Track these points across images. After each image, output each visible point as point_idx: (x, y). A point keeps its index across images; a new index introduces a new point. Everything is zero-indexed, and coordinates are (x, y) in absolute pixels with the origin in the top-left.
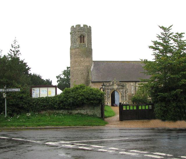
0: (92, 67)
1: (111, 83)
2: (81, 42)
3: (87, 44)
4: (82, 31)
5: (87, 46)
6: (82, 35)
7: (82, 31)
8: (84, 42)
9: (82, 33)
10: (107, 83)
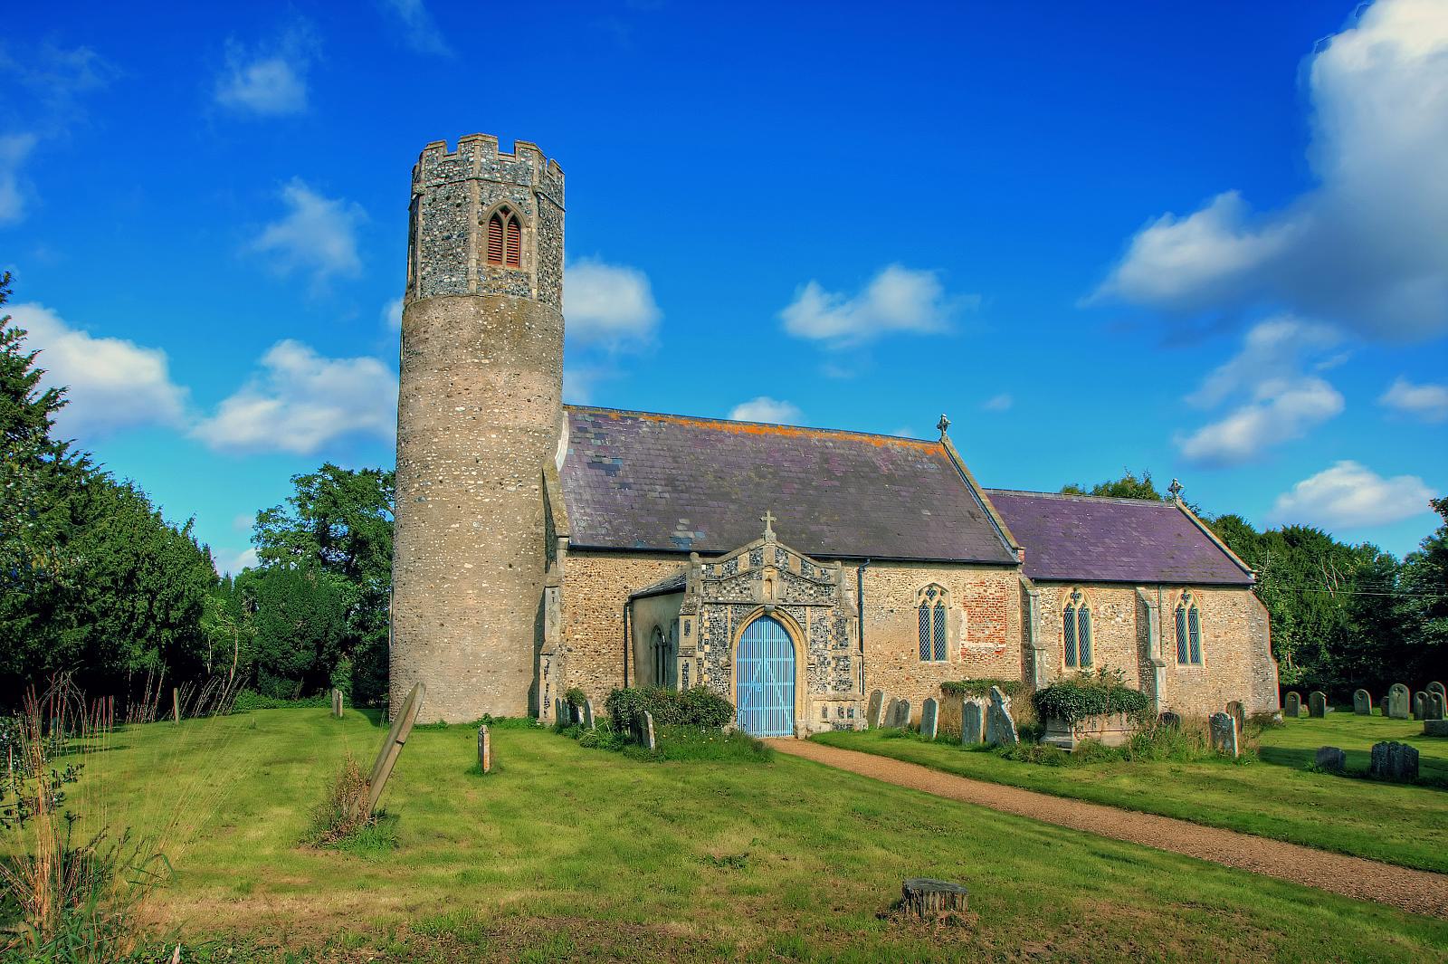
0: (563, 447)
1: (744, 563)
2: (494, 257)
3: (534, 278)
4: (507, 184)
5: (534, 292)
6: (505, 210)
7: (507, 184)
8: (514, 261)
9: (505, 197)
10: (709, 560)
